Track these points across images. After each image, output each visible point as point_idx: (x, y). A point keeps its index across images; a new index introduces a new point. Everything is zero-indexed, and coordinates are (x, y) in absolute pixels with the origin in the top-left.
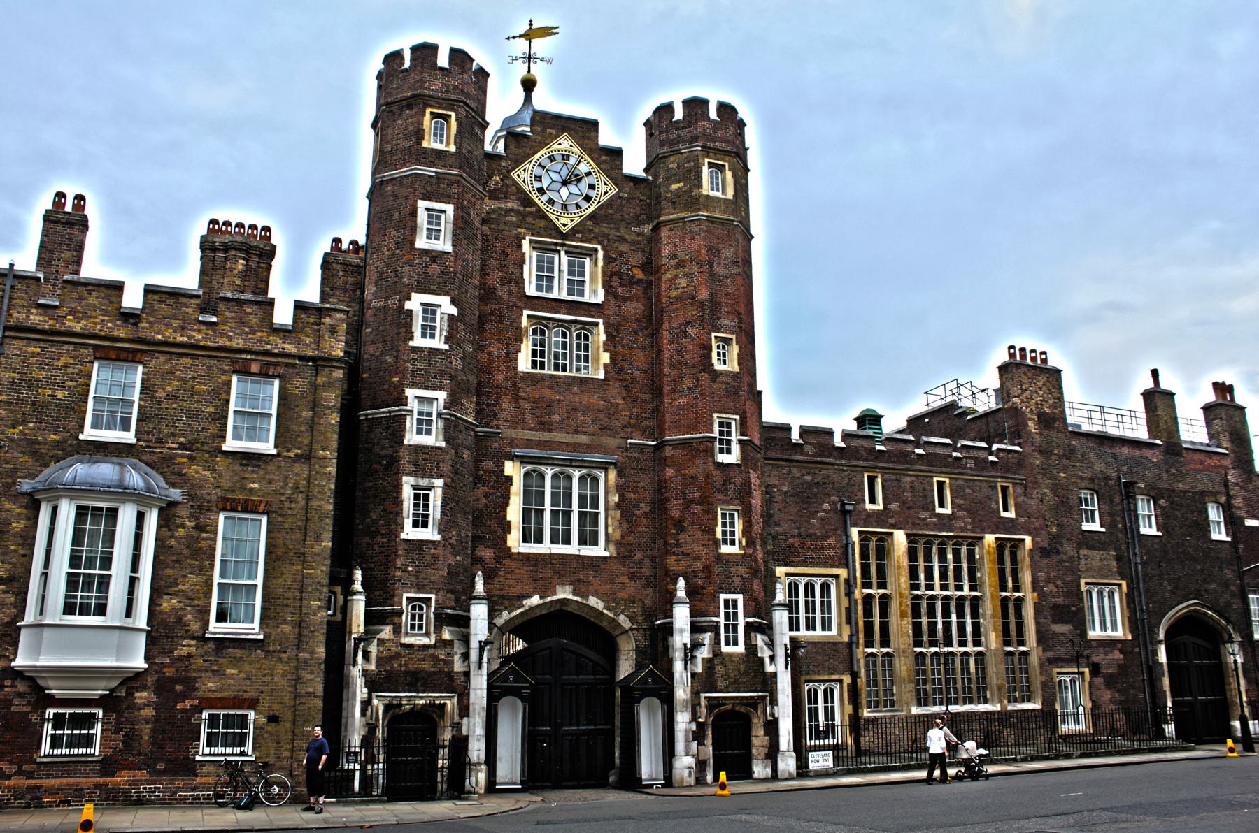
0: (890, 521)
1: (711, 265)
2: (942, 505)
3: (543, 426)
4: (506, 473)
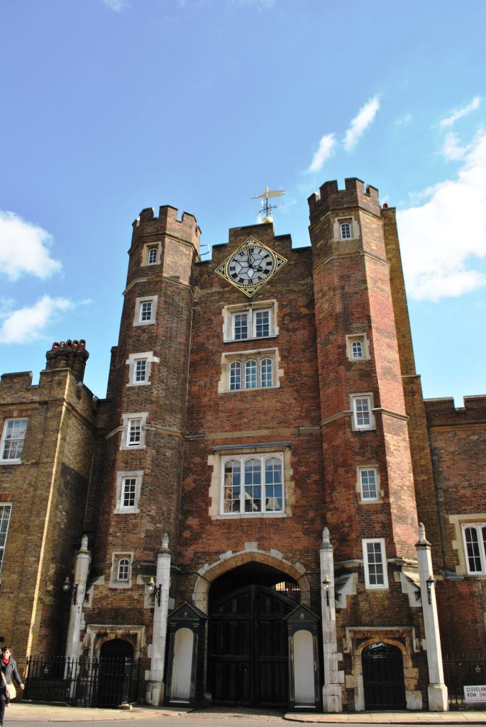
1: (343, 288)
3: (236, 427)
4: (209, 464)
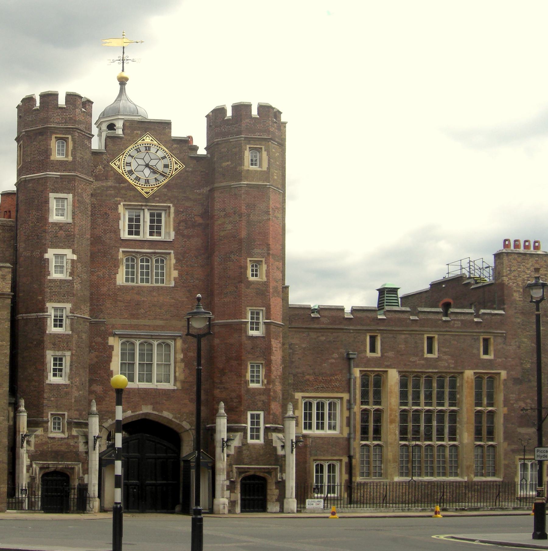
0: (386, 363)
2: (430, 351)
